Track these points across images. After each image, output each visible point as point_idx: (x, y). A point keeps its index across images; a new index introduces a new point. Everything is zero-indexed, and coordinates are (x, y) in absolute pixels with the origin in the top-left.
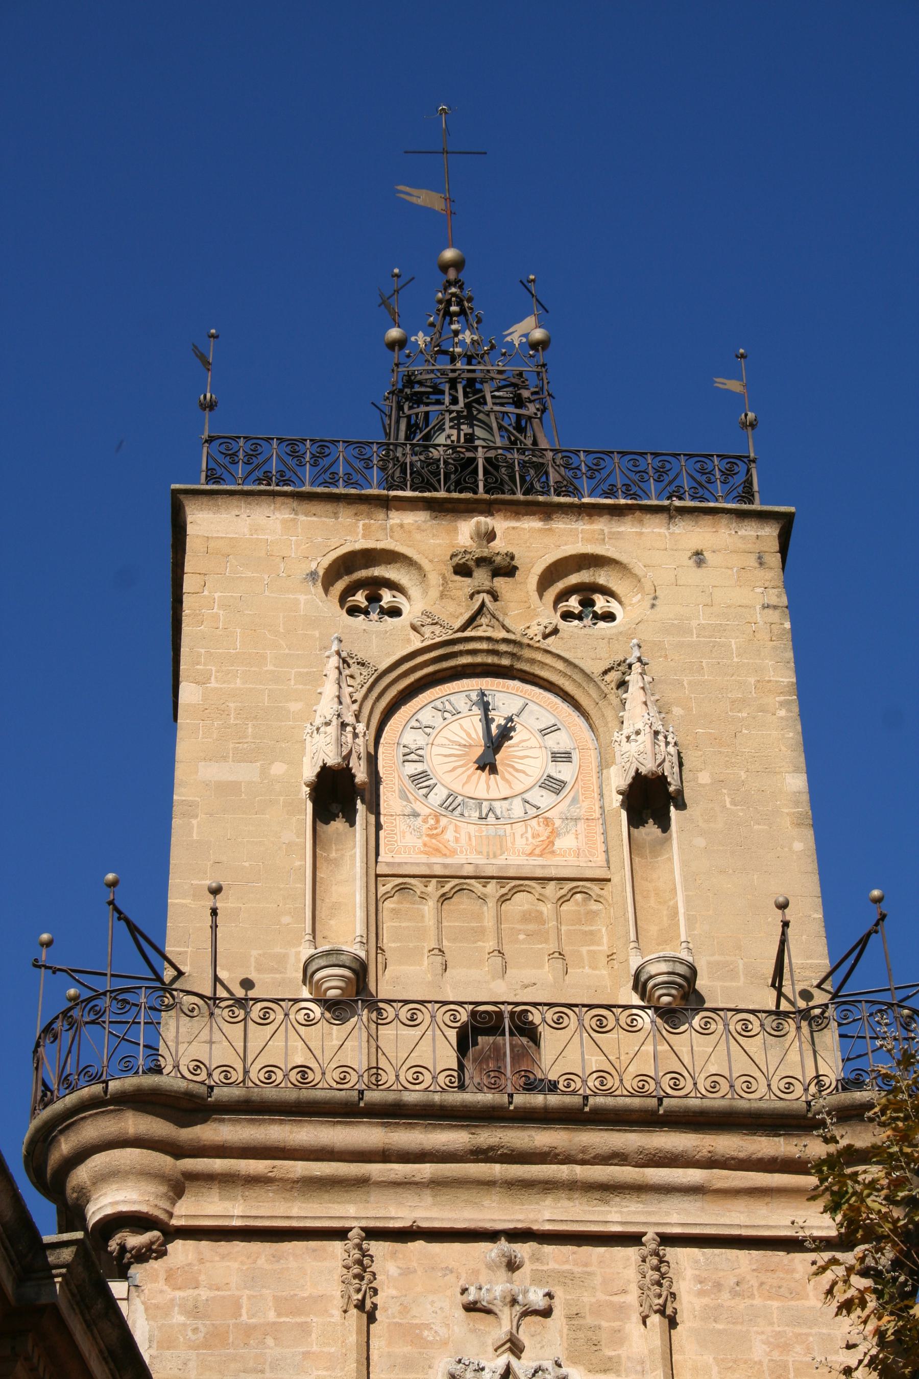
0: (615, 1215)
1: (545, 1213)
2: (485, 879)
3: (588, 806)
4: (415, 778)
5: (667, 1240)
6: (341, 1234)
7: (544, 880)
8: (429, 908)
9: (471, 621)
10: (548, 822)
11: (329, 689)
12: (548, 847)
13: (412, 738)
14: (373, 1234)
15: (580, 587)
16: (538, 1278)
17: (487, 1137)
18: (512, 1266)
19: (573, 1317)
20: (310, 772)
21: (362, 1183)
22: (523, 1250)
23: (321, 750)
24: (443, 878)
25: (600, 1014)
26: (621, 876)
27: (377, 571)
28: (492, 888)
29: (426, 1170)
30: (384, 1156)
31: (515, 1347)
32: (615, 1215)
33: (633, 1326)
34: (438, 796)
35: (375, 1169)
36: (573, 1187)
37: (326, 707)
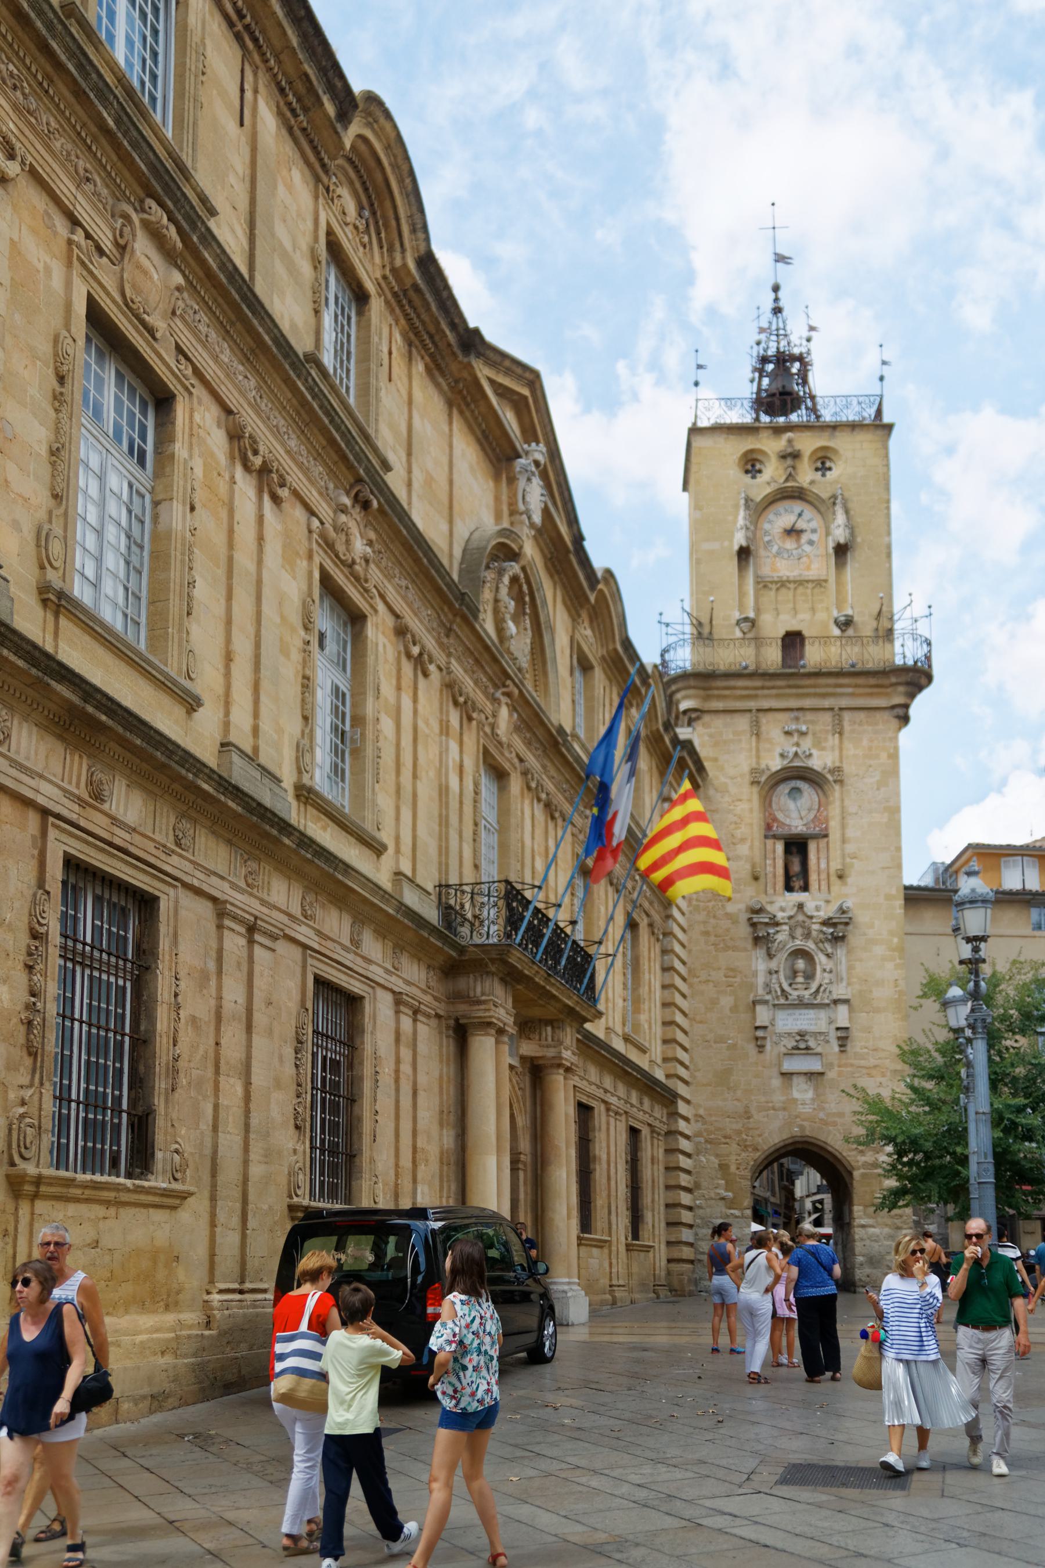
0: (827, 703)
1: (807, 703)
2: (789, 582)
3: (821, 551)
4: (769, 542)
5: (841, 709)
6: (750, 711)
7: (807, 581)
8: (773, 593)
9: (787, 480)
10: (808, 556)
11: (742, 513)
12: (808, 568)
13: (767, 526)
14: (758, 710)
15: (823, 462)
16: (805, 722)
17: (792, 682)
18: (797, 719)
19: (814, 734)
20: (736, 548)
21: (756, 696)
22: (800, 714)
23: (739, 539)
24: (776, 583)
25: (825, 639)
26: (832, 579)
27: (755, 456)
28: (792, 586)
29: (774, 692)
30: (763, 688)
31: (798, 745)
32: (827, 703)
33: (830, 737)
34: (775, 549)
35: (760, 692)
36: (815, 695)
37: (741, 521)
